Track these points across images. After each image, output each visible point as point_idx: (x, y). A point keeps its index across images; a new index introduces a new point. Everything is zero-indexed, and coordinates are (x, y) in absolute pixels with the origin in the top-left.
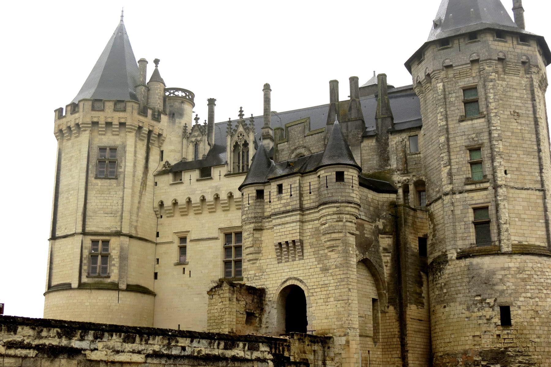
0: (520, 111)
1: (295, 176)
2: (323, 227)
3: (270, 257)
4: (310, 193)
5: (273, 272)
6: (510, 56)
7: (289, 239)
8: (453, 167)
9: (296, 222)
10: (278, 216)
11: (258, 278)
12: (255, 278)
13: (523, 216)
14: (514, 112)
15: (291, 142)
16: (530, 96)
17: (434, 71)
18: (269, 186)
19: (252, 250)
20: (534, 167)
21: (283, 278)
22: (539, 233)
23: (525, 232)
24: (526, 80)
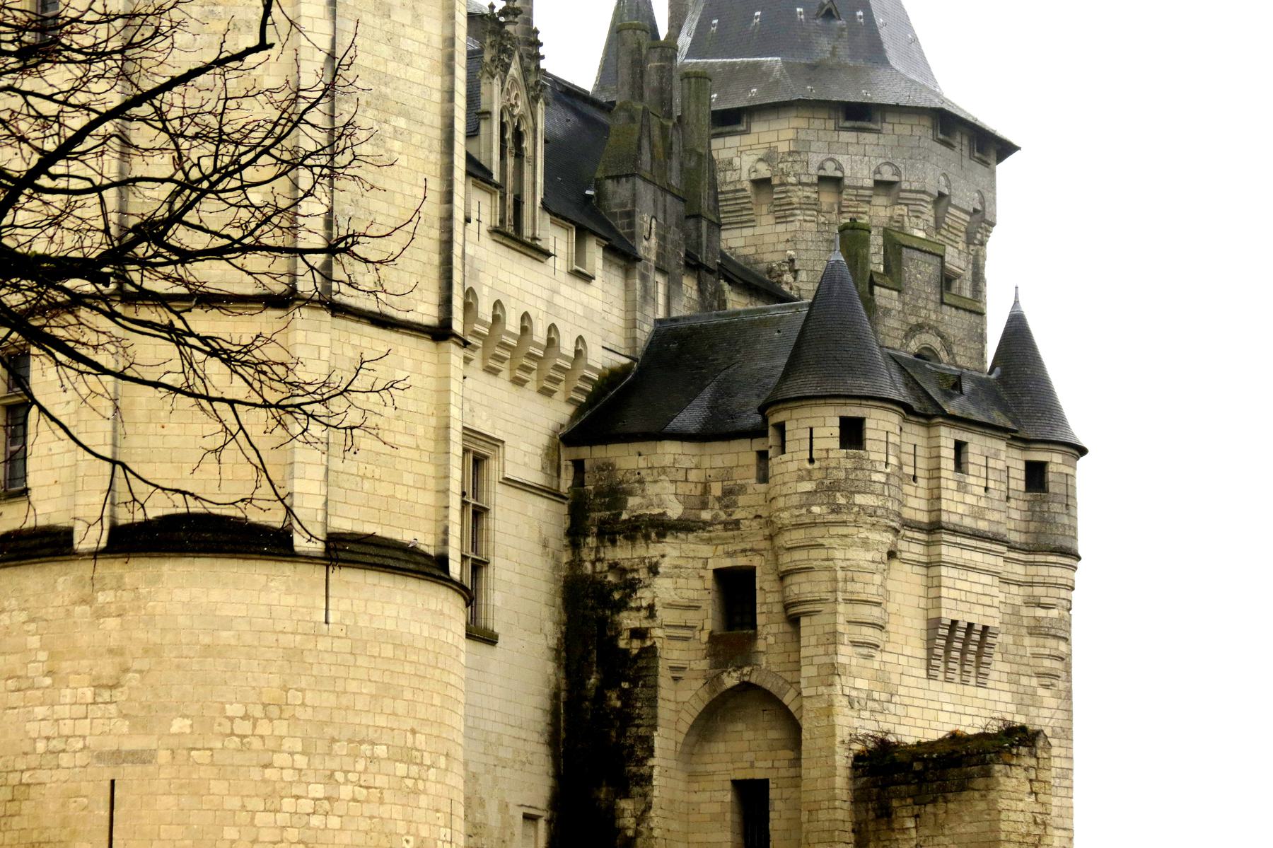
1: (999, 438)
2: (1041, 613)
3: (908, 651)
4: (1008, 498)
5: (916, 702)
7: (979, 622)
9: (995, 574)
10: (959, 540)
11: (876, 706)
12: (870, 704)
15: (907, 298)
17: (924, 192)
18: (916, 429)
19: (876, 611)
21: (940, 726)
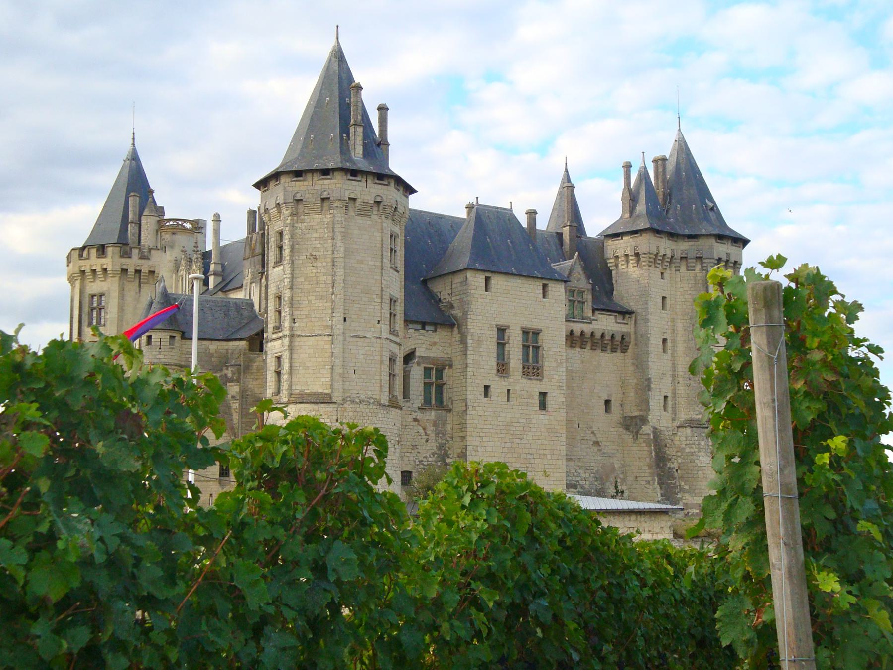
0: (317, 253)
6: (307, 195)
8: (269, 315)
13: (307, 364)
14: (312, 255)
16: (331, 235)
20: (325, 311)
22: (323, 379)
23: (308, 380)
24: (329, 216)
